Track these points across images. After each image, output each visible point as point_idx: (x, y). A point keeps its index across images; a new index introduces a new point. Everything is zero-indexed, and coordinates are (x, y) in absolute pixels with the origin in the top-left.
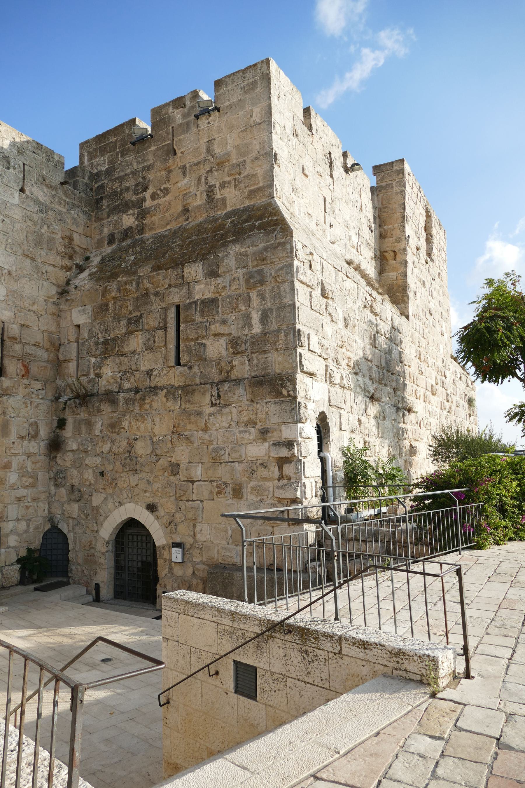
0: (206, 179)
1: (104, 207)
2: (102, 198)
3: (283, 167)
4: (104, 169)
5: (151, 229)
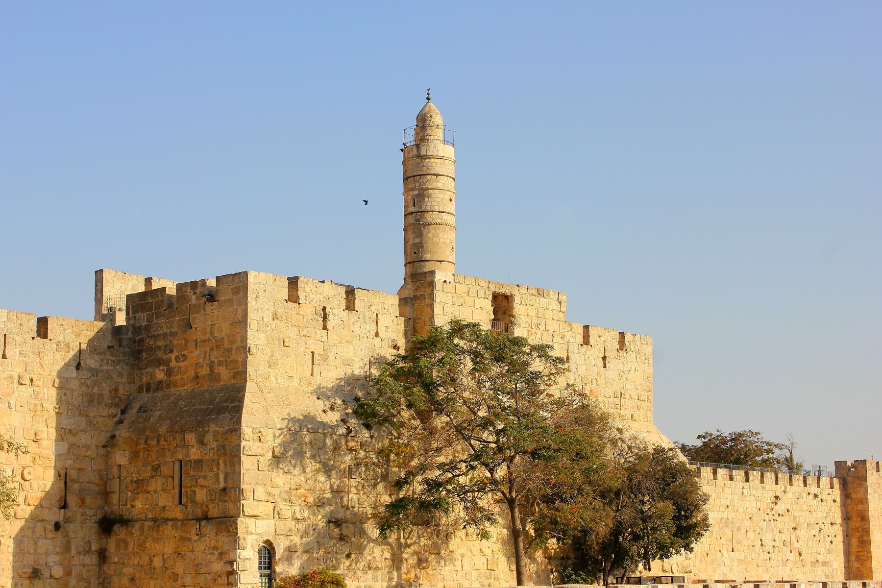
4: (143, 324)
5: (175, 386)
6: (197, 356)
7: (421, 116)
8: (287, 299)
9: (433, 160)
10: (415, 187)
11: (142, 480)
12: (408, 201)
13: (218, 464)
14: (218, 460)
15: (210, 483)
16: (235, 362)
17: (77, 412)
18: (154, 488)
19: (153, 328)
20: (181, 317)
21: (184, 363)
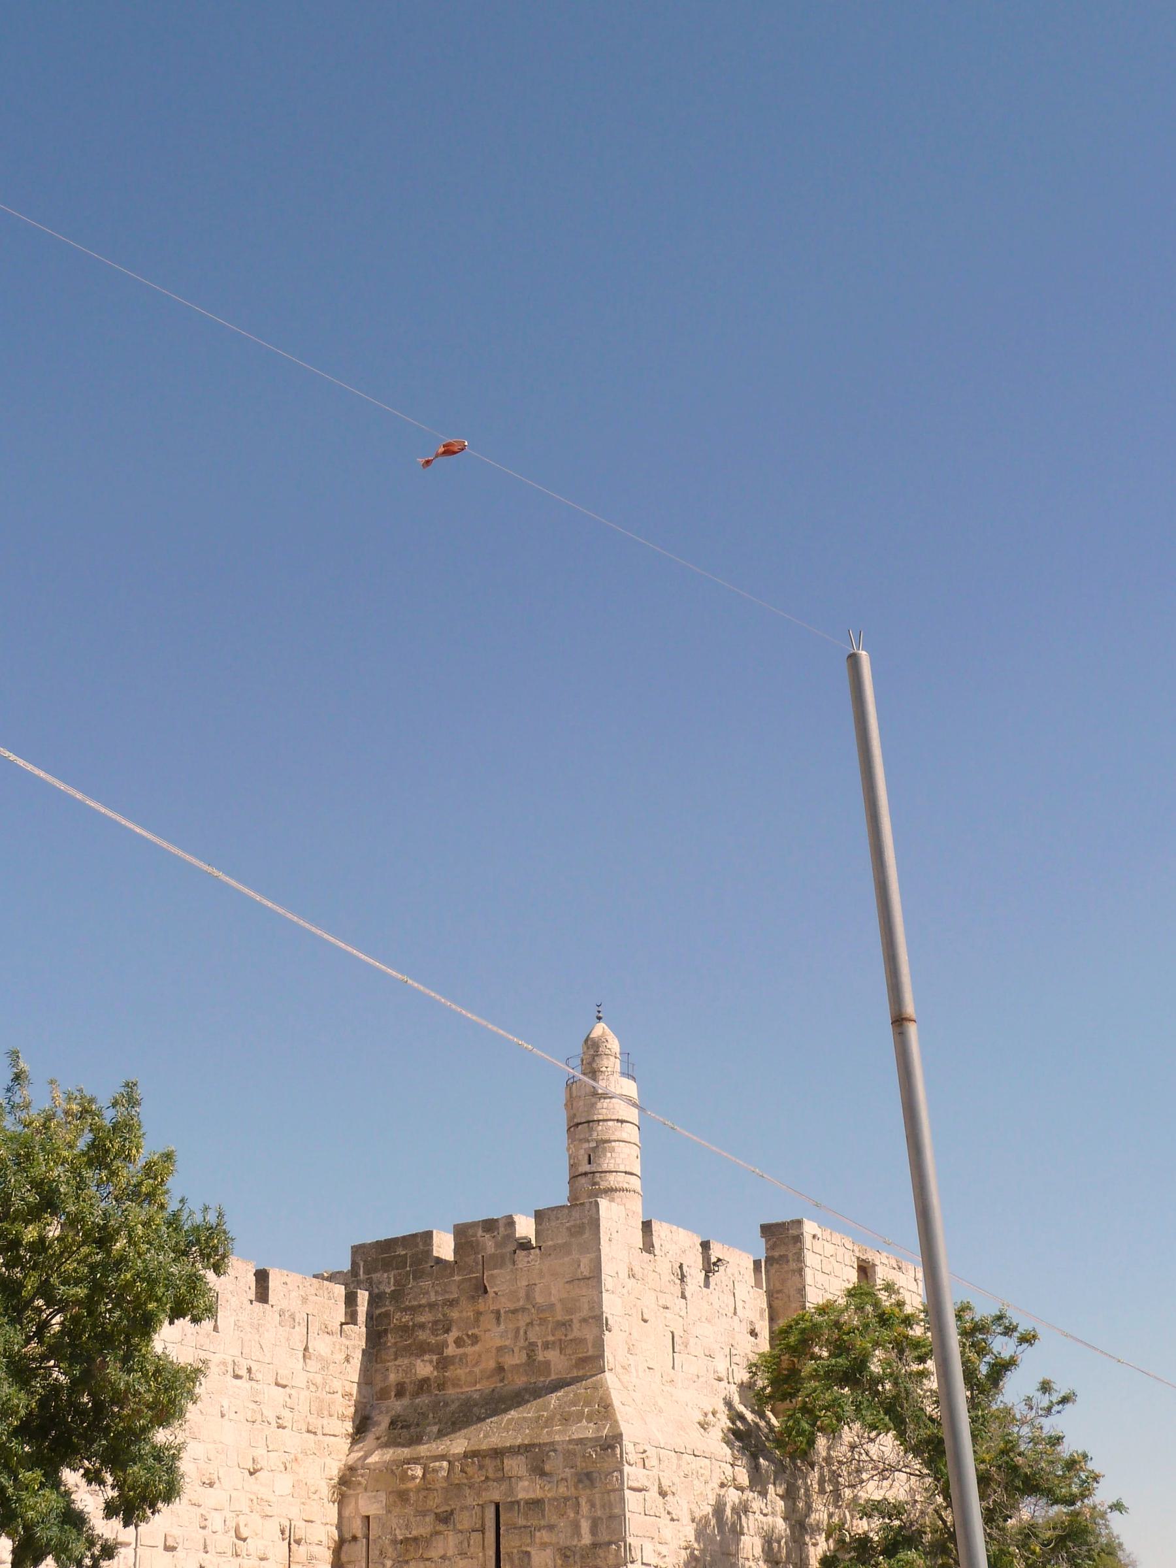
0: (526, 1333)
1: (389, 1344)
2: (386, 1331)
3: (615, 1329)
4: (388, 1290)
8: (642, 1247)
11: (415, 1539)
13: (578, 1504)
14: (577, 1498)
15: (562, 1538)
16: (580, 1341)
17: (304, 1428)
18: (442, 1552)
19: (409, 1294)
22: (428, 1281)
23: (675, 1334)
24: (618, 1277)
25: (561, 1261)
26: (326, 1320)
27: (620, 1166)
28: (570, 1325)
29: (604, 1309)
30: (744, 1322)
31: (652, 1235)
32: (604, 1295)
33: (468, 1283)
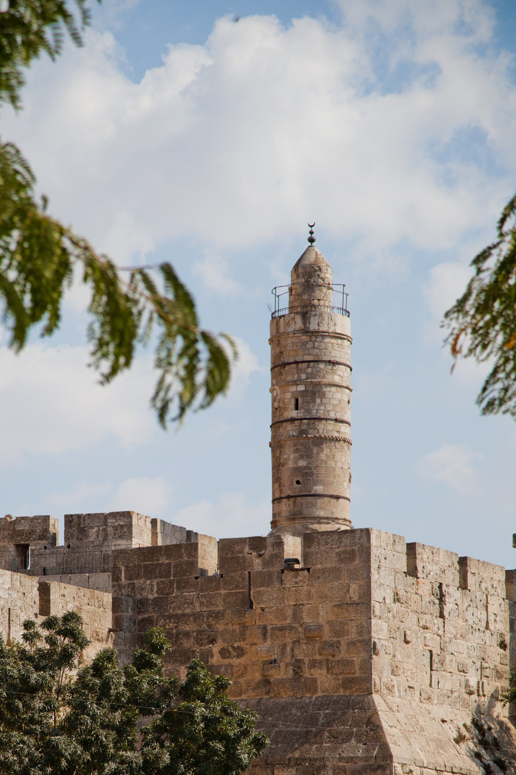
3: (382, 652)
4: (151, 597)
6: (268, 651)
7: (304, 267)
8: (406, 571)
9: (327, 340)
10: (300, 379)
12: (286, 400)
16: (349, 663)
19: (173, 602)
20: (232, 589)
21: (239, 660)
22: (193, 592)
23: (434, 652)
24: (385, 602)
25: (330, 585)
26: (97, 628)
27: (331, 413)
28: (337, 647)
29: (373, 634)
30: (495, 635)
31: (415, 558)
32: (373, 621)
33: (235, 598)
